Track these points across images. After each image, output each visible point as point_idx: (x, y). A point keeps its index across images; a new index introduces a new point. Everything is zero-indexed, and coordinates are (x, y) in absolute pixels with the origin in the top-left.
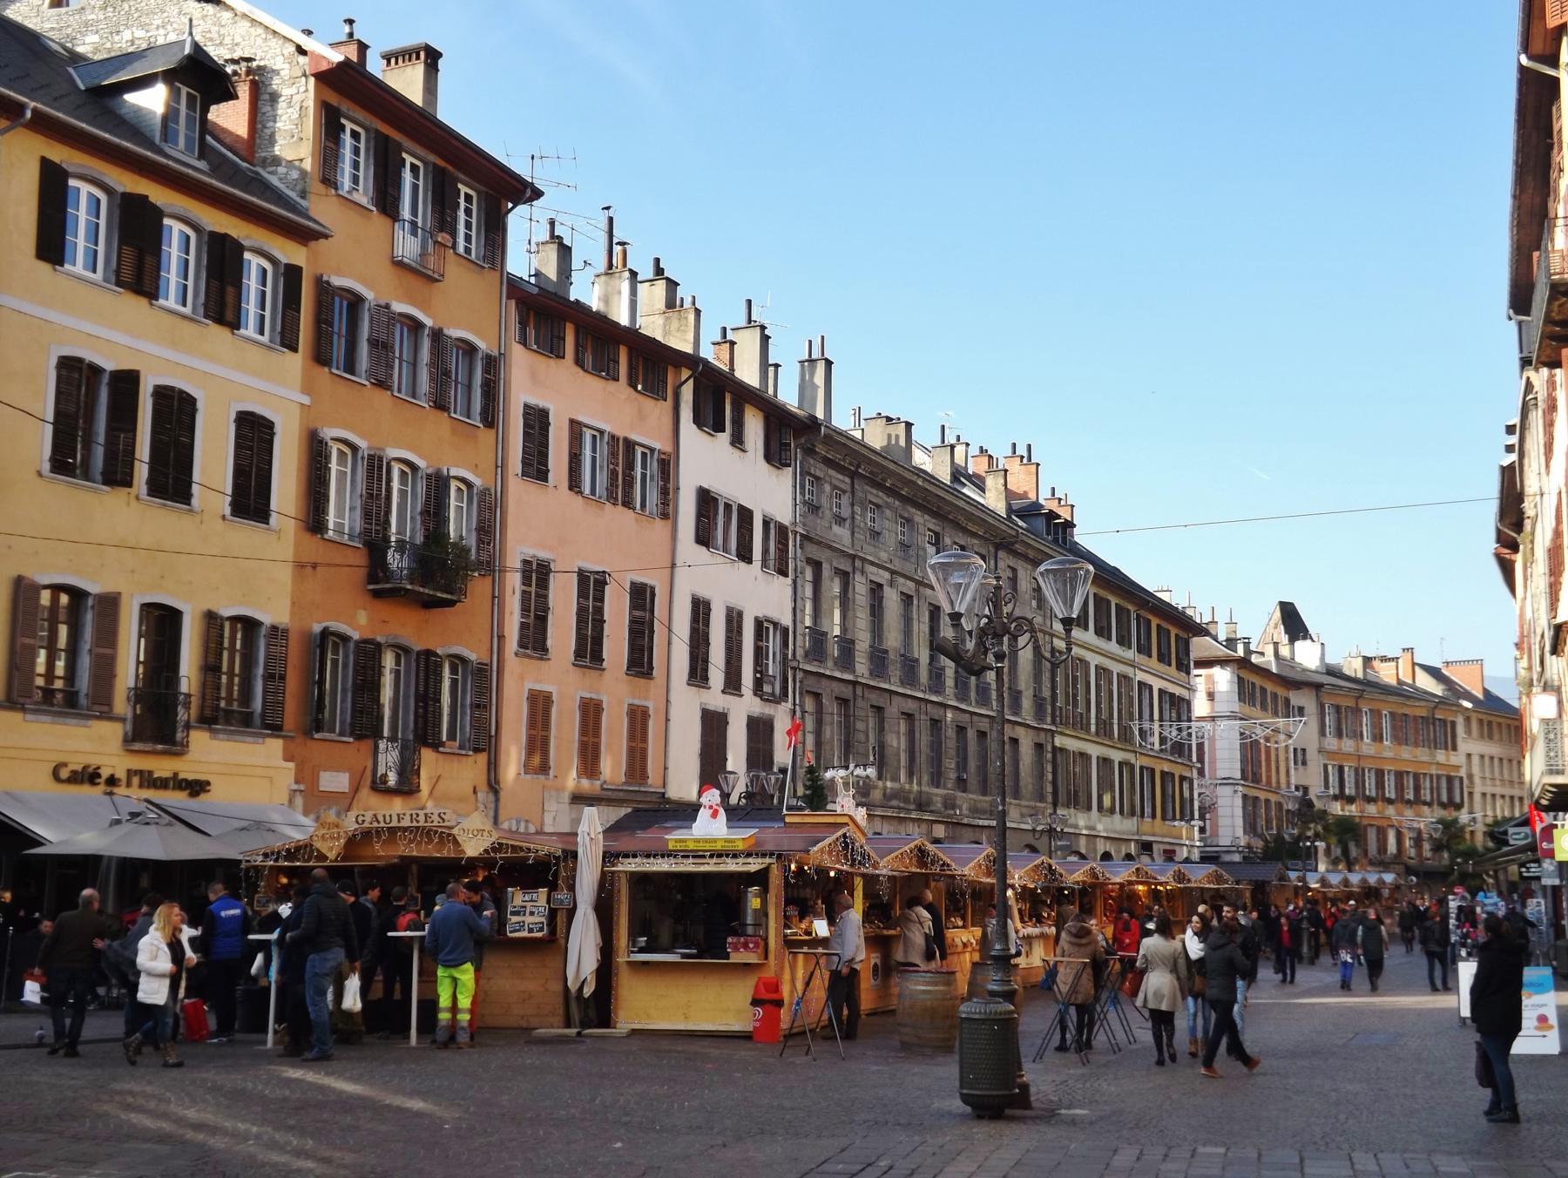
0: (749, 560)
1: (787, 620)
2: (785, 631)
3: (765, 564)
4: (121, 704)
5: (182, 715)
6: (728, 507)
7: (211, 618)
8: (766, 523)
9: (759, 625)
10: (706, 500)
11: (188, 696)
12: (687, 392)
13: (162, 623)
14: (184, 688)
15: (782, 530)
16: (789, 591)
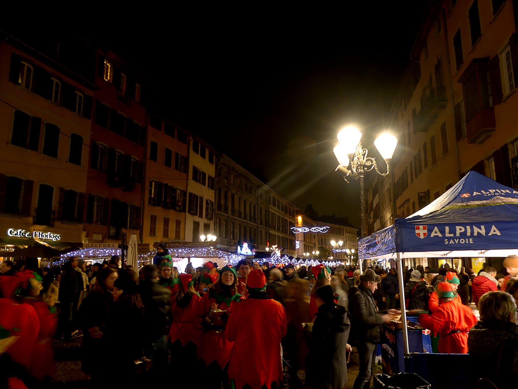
0: (205, 185)
1: (213, 201)
2: (213, 203)
3: (208, 187)
4: (33, 212)
5: (52, 216)
6: (200, 172)
7: (61, 190)
8: (209, 177)
9: (207, 201)
10: (195, 168)
11: (54, 211)
12: (191, 142)
13: (46, 191)
14: (53, 209)
15: (212, 178)
16: (214, 193)
